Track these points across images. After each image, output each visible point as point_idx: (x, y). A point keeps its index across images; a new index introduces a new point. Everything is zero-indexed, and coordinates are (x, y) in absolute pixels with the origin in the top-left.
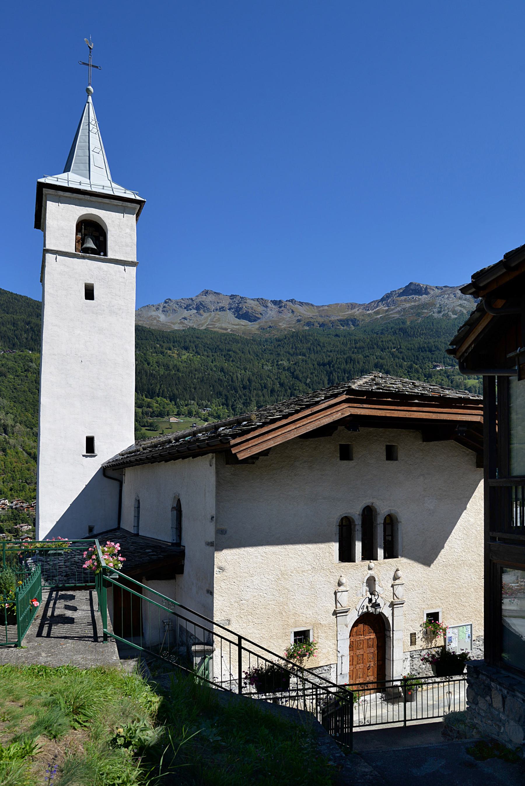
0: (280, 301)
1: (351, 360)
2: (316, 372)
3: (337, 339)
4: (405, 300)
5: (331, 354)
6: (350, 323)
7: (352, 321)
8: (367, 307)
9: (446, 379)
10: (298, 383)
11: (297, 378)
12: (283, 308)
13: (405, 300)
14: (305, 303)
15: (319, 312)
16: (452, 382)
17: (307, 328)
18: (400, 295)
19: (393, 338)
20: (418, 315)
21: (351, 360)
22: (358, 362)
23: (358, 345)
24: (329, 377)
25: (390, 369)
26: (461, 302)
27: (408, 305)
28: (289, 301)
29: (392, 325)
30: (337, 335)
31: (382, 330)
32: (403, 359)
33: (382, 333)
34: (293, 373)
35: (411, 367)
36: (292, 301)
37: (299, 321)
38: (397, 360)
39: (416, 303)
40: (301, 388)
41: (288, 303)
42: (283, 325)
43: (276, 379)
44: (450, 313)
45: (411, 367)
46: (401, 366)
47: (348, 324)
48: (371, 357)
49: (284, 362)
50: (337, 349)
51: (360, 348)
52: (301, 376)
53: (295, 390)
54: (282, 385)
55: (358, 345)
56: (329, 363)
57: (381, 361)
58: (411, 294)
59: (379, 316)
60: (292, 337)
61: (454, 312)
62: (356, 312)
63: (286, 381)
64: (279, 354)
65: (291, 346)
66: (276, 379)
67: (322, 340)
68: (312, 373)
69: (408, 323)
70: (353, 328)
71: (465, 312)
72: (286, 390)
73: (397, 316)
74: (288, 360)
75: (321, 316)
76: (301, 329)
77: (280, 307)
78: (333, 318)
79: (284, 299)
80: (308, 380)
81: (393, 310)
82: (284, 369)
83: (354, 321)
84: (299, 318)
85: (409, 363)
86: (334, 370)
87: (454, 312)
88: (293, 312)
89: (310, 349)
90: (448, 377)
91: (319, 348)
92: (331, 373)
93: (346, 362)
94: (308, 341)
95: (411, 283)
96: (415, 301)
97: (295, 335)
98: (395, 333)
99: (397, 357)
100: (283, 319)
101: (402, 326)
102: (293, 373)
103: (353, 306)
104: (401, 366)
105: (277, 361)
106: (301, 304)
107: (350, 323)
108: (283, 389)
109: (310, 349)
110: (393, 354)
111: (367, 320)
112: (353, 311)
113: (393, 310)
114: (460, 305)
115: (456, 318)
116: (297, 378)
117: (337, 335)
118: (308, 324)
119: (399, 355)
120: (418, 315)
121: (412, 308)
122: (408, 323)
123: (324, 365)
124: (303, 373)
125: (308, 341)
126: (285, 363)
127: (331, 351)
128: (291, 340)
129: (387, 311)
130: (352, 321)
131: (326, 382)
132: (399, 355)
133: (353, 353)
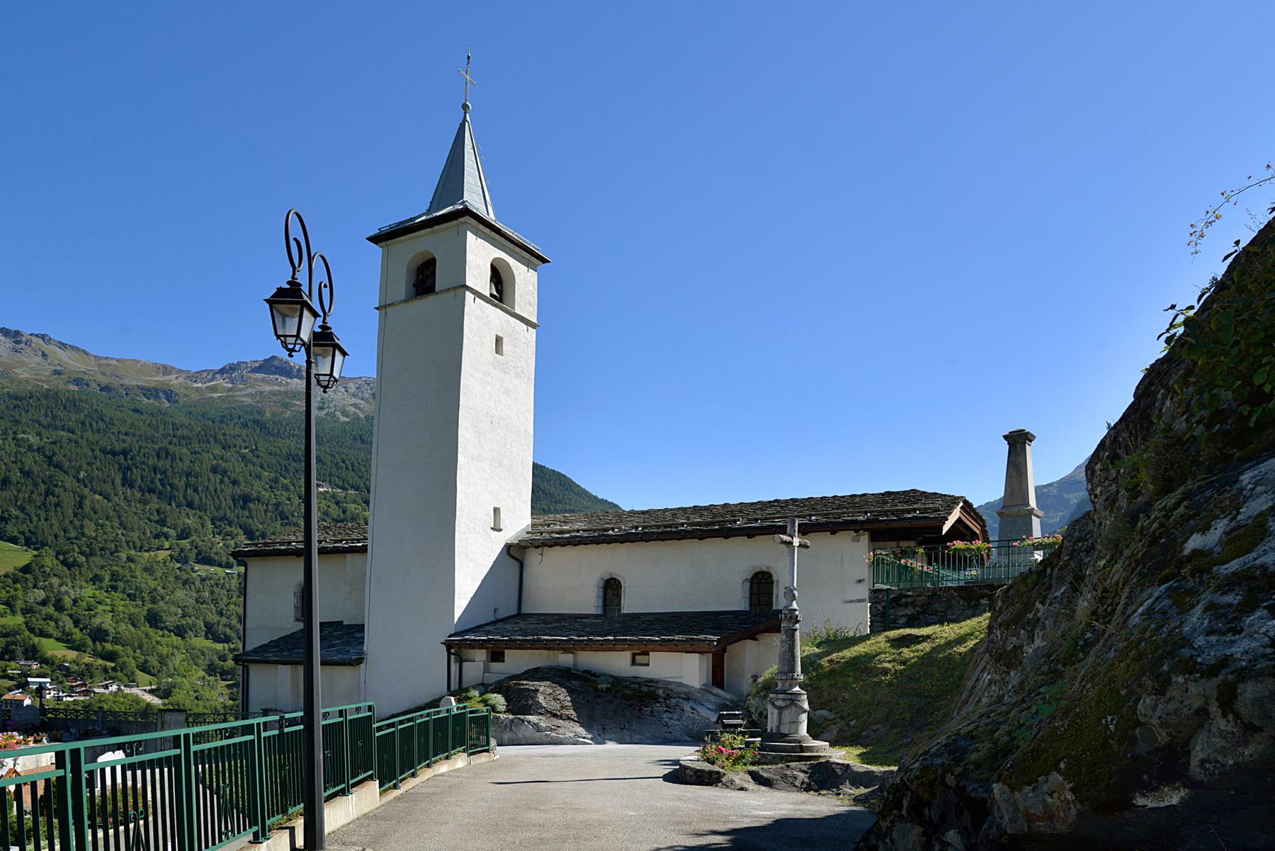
0: (17, 333)
1: (167, 453)
2: (98, 463)
3: (137, 415)
4: (263, 380)
5: (129, 439)
6: (161, 395)
7: (165, 393)
8: (194, 377)
9: (333, 506)
10: (61, 476)
11: (59, 466)
12: (22, 345)
13: (263, 380)
14: (72, 347)
15: (100, 366)
16: (344, 512)
17: (76, 388)
18: (254, 370)
19: (244, 432)
20: (286, 406)
21: (167, 453)
22: (181, 459)
23: (179, 433)
24: (125, 474)
25: (241, 479)
26: (354, 400)
27: (267, 388)
28: (37, 336)
29: (239, 412)
30: (136, 410)
31: (223, 417)
32: (262, 467)
33: (222, 422)
34: (50, 458)
35: (276, 481)
36: (43, 337)
37: (57, 373)
38: (251, 467)
39: (282, 389)
40: (67, 485)
41: (34, 339)
42: (22, 373)
43: (15, 462)
44: (338, 414)
45: (276, 481)
46: (259, 477)
47: (156, 397)
48: (206, 455)
49: (30, 437)
50: (138, 433)
51: (183, 438)
52: (66, 464)
53: (56, 486)
54: (26, 474)
55: (179, 433)
56: (125, 453)
57: (224, 464)
58: (273, 373)
59: (216, 395)
60: (46, 397)
61: (345, 413)
62: (174, 381)
63: (36, 469)
64: (17, 422)
65: (43, 412)
66: (15, 462)
67: (109, 413)
68: (89, 464)
69: (268, 415)
70: (167, 404)
71: (362, 416)
72: (36, 485)
73: (248, 401)
74: (39, 434)
75: (105, 374)
76: (62, 386)
77: (18, 342)
78: (126, 382)
79: (26, 330)
80: (82, 475)
81: (241, 390)
82: (30, 447)
83: (169, 394)
84: (58, 368)
85: (273, 475)
86: (135, 464)
87: (345, 413)
88: (44, 355)
89: (83, 424)
90: (337, 503)
91: (102, 425)
92: (128, 468)
93: (158, 456)
94: (78, 410)
95: (273, 357)
96: (280, 384)
97: (52, 396)
98: (245, 425)
99: (250, 461)
100: (24, 364)
101: (257, 417)
102: (50, 458)
103: (166, 370)
104: (259, 477)
105: (15, 433)
106: (63, 346)
107: (161, 395)
108: (29, 482)
109: (83, 424)
110: (243, 457)
111: (194, 397)
112: (166, 378)
113: (241, 390)
114: (355, 405)
115: (347, 423)
116: (59, 466)
117: (136, 410)
118: (77, 382)
119: (254, 459)
120: (286, 406)
121: (275, 394)
122: (268, 415)
123: (114, 453)
124: (70, 461)
125: (78, 410)
126: (33, 439)
127: (126, 434)
128: (45, 402)
129: (230, 390)
130: (165, 393)
131: (118, 481)
132: (254, 459)
133: (170, 443)
